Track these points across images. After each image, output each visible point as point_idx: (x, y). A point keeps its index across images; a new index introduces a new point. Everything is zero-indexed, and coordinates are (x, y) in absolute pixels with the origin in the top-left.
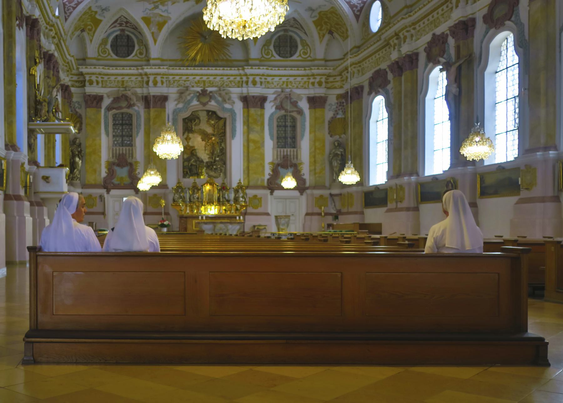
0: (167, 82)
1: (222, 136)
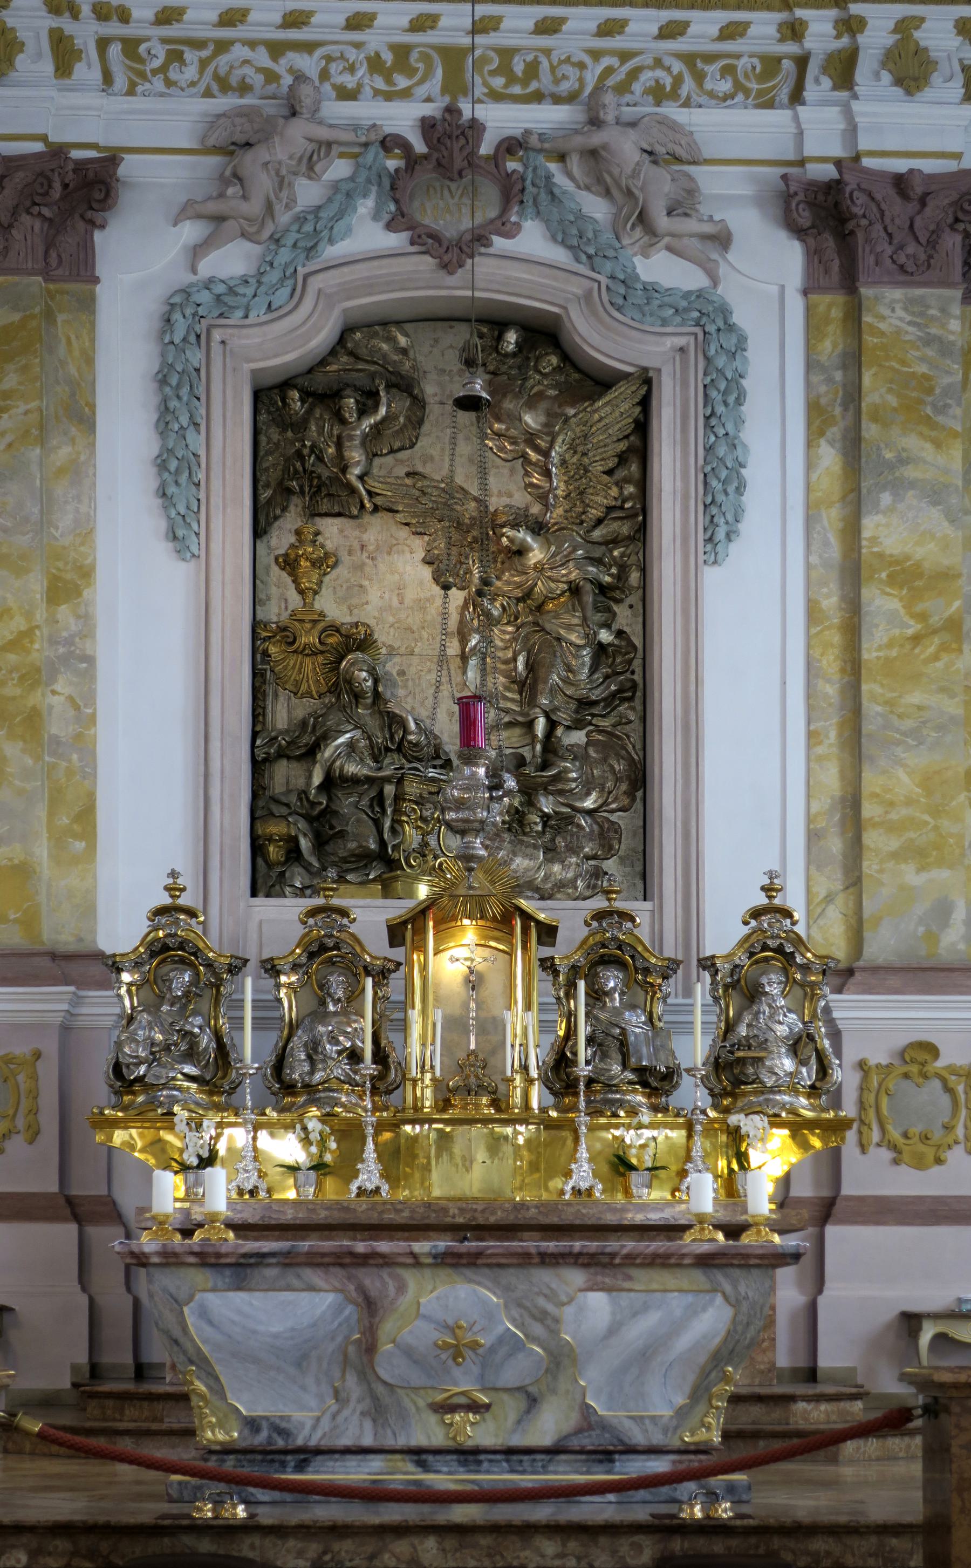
0: (115, 50)
1: (614, 541)
